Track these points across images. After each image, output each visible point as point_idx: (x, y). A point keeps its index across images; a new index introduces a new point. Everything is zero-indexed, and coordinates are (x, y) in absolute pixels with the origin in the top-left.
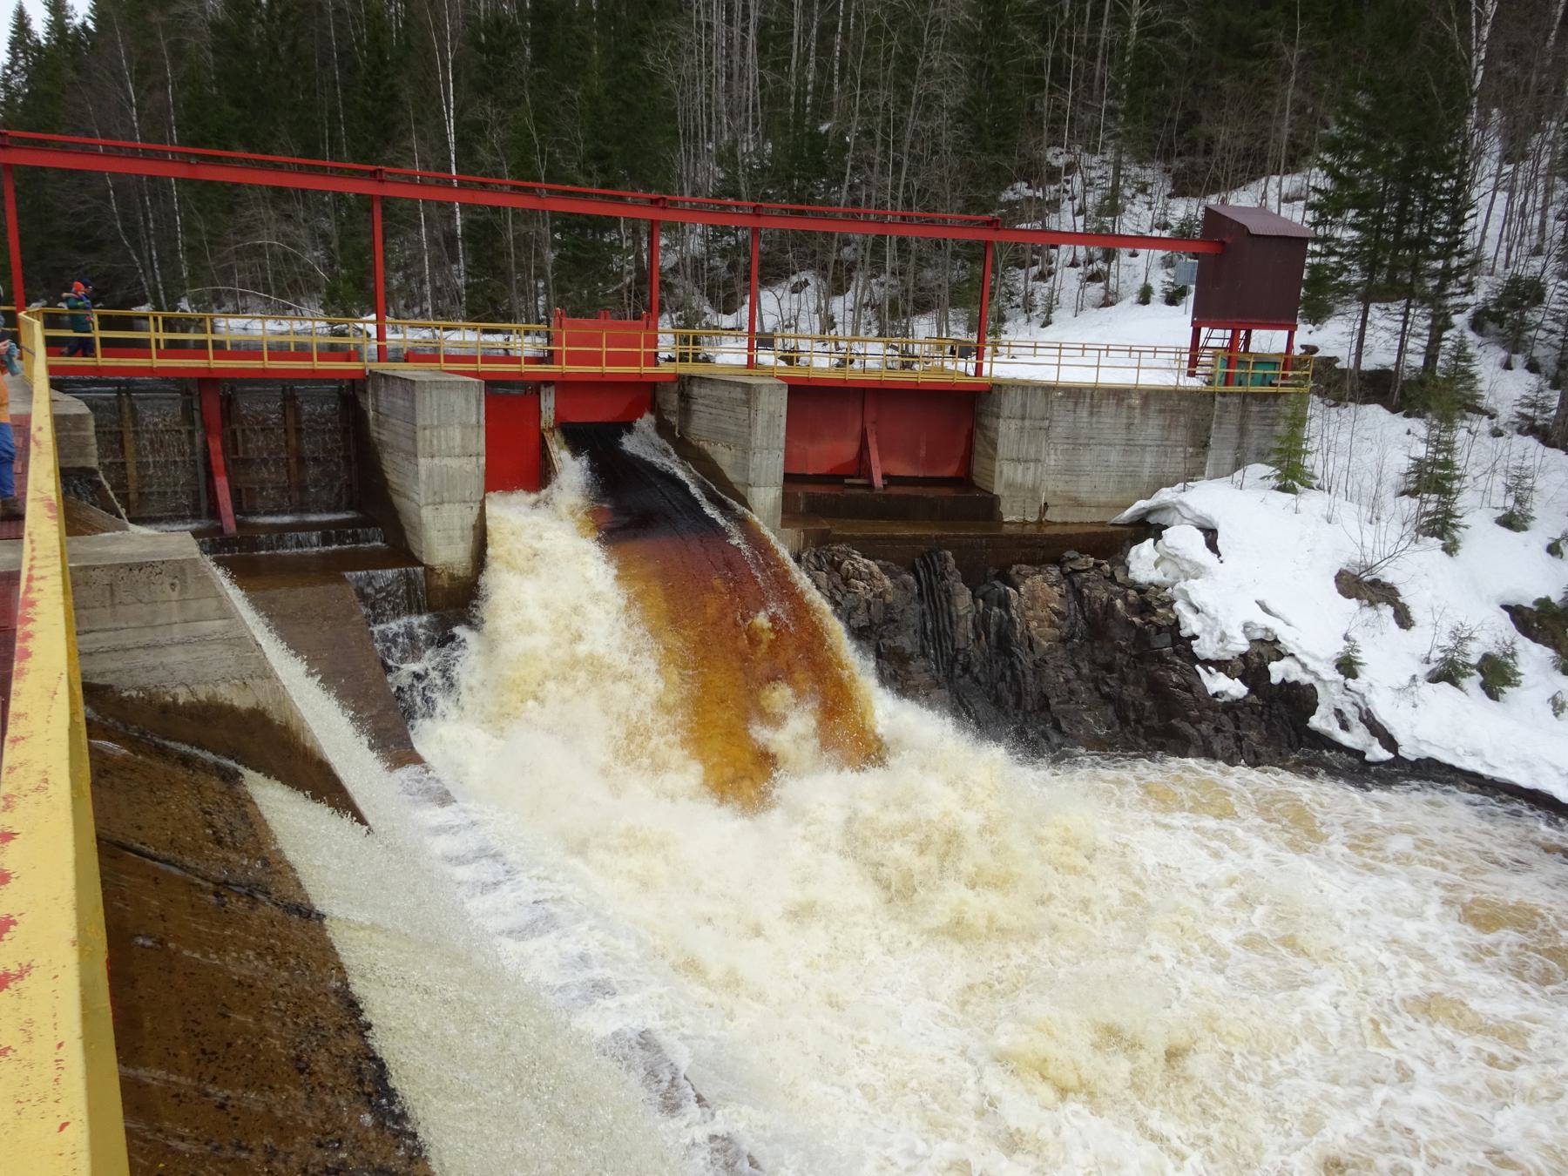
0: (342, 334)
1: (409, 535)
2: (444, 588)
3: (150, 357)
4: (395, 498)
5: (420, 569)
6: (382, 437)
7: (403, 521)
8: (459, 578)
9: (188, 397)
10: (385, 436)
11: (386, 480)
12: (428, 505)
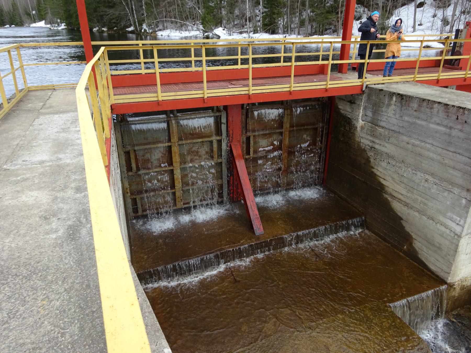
0: (208, 38)
1: (418, 245)
2: (454, 296)
3: (202, 89)
4: (397, 206)
5: (444, 287)
6: (377, 146)
7: (408, 228)
8: (468, 286)
9: (218, 114)
10: (388, 148)
11: (382, 187)
12: (467, 235)
